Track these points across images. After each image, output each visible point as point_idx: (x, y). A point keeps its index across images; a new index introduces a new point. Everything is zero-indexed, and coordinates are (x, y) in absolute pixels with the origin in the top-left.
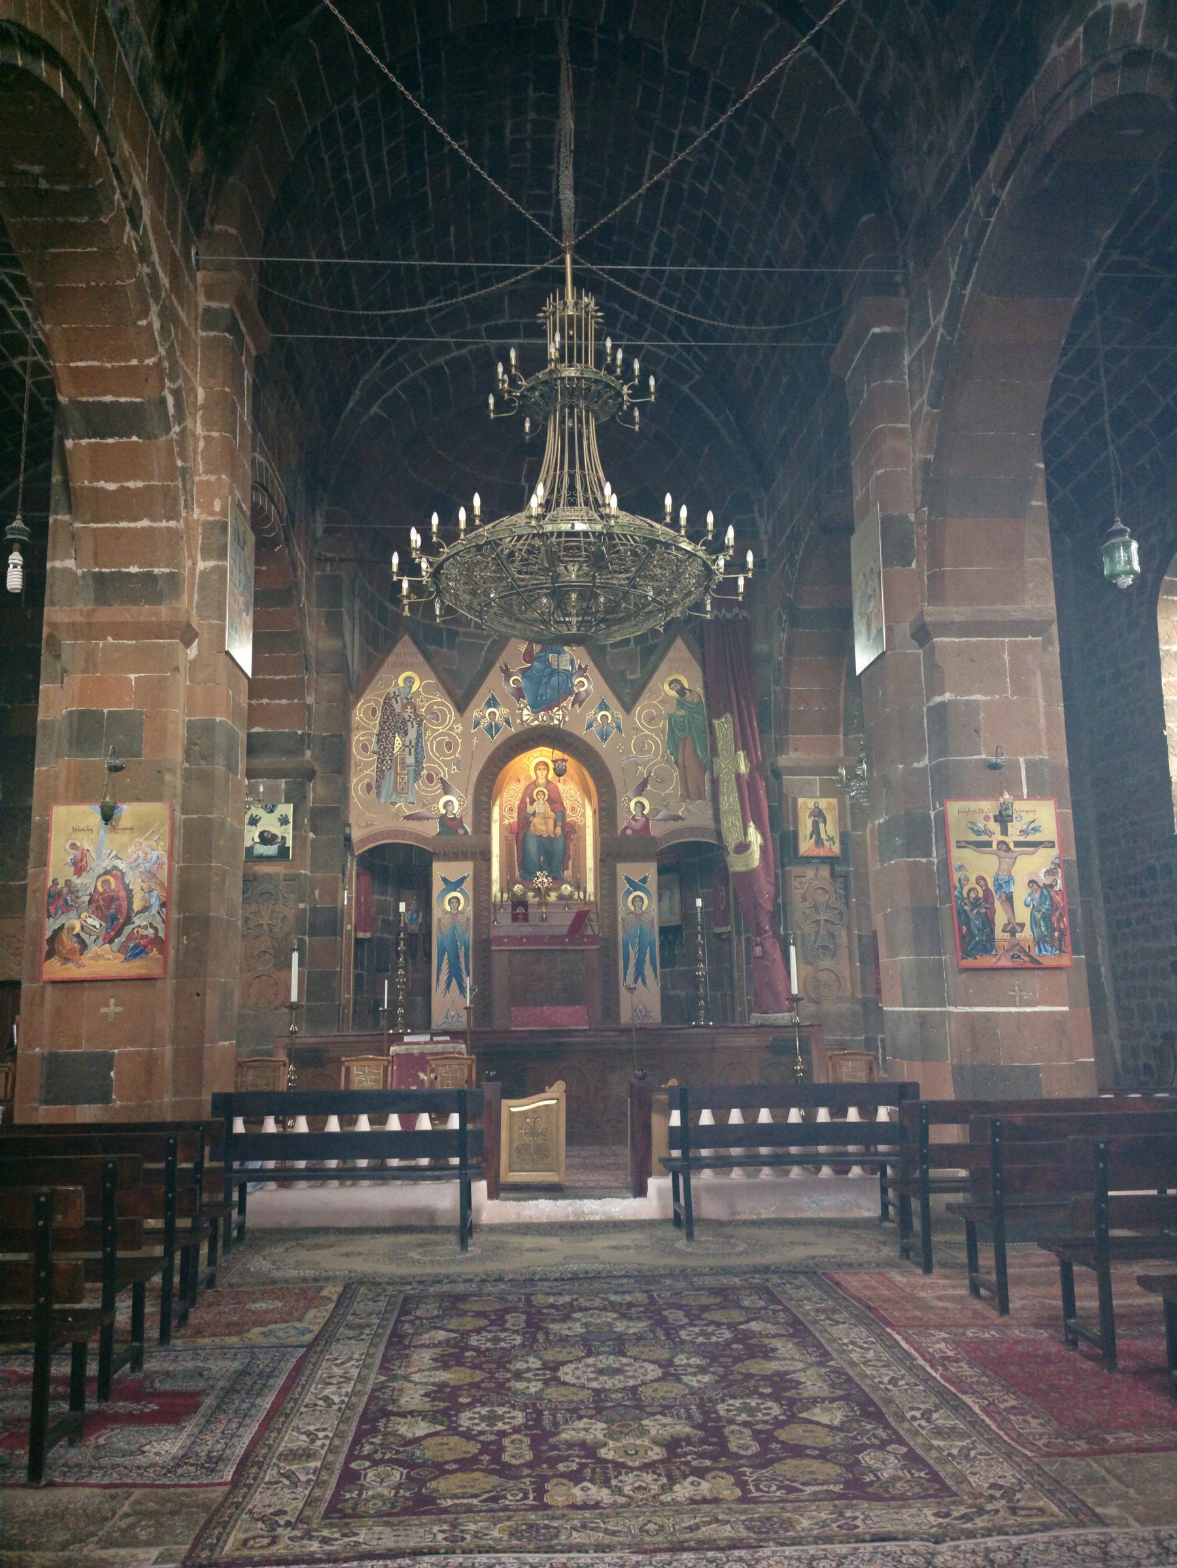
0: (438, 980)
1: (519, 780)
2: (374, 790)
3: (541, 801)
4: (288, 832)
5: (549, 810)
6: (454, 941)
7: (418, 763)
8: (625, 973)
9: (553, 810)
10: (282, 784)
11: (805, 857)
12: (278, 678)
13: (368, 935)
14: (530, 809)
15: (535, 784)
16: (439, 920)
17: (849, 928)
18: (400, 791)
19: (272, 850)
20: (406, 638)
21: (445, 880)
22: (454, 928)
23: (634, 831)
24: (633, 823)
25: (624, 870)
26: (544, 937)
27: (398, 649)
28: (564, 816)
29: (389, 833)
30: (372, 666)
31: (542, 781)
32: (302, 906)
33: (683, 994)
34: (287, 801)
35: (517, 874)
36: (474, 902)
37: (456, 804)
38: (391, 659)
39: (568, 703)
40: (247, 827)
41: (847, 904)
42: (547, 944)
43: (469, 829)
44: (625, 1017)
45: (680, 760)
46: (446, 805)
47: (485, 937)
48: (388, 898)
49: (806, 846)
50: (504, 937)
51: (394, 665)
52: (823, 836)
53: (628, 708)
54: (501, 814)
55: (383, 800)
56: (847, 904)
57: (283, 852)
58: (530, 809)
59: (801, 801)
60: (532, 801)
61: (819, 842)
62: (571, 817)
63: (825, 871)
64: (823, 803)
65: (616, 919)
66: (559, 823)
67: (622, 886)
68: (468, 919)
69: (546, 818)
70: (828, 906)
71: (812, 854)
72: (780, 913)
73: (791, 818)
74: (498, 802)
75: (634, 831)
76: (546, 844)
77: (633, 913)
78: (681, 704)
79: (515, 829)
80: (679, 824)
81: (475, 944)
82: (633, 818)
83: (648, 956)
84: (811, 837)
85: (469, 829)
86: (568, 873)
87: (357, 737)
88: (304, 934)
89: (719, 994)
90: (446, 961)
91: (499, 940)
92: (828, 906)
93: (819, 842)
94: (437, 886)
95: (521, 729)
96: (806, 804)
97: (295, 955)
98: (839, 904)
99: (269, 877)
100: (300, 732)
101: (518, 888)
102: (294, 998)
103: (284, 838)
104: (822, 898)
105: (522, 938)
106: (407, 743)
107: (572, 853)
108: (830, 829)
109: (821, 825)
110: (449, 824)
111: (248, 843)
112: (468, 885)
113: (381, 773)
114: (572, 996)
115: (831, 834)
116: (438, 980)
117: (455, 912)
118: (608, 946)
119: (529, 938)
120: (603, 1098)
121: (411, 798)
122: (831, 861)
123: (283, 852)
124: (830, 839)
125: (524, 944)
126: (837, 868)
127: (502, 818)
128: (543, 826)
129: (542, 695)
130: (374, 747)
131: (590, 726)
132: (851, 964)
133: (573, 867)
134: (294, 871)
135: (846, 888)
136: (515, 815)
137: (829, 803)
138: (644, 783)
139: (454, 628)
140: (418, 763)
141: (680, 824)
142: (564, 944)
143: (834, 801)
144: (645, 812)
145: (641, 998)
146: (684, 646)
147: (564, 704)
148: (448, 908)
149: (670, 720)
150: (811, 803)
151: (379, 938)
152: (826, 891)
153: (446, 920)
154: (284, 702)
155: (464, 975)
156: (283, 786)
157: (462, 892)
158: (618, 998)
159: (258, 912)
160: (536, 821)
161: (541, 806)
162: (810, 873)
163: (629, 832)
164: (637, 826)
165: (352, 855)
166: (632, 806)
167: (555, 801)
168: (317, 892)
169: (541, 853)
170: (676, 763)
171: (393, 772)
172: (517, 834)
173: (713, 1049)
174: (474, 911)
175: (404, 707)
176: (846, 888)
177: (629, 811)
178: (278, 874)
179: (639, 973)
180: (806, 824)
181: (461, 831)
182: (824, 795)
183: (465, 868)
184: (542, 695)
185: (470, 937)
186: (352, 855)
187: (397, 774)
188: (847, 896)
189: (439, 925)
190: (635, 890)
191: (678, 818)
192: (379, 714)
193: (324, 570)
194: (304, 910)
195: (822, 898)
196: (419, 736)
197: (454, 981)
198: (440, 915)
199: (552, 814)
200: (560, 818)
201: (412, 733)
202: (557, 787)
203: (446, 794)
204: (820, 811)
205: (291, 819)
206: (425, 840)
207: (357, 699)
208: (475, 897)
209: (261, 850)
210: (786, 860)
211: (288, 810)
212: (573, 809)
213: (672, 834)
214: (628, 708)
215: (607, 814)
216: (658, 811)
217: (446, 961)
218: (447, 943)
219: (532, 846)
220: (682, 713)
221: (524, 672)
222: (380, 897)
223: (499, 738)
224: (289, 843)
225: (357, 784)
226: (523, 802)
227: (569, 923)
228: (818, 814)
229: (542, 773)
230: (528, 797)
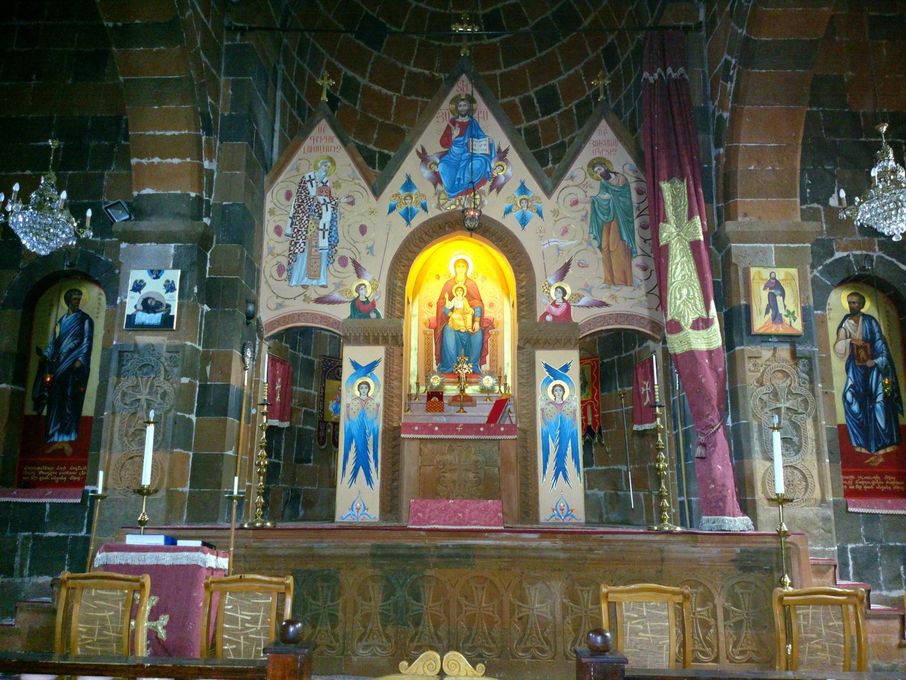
0: (344, 469)
1: (438, 277)
2: (285, 275)
3: (460, 297)
4: (173, 300)
5: (467, 305)
6: (363, 427)
7: (333, 245)
8: (545, 468)
9: (471, 306)
10: (171, 248)
11: (762, 335)
12: (169, 133)
13: (286, 424)
14: (449, 305)
15: (454, 281)
16: (348, 406)
17: (816, 420)
18: (313, 272)
19: (155, 318)
20: (324, 122)
21: (355, 365)
22: (363, 414)
23: (553, 316)
24: (554, 309)
25: (543, 357)
26: (457, 425)
27: (315, 133)
28: (482, 312)
29: (299, 316)
30: (289, 150)
31: (461, 278)
32: (185, 380)
33: (601, 494)
34: (175, 267)
35: (435, 367)
36: (385, 388)
37: (372, 287)
38: (308, 142)
39: (486, 188)
40: (131, 294)
41: (812, 390)
42: (461, 433)
43: (382, 313)
44: (546, 515)
45: (604, 246)
46: (357, 290)
47: (395, 425)
48: (312, 392)
49: (761, 322)
50: (415, 425)
51: (310, 149)
52: (782, 311)
53: (548, 193)
54: (420, 307)
55: (294, 283)
56: (812, 390)
57: (167, 321)
58: (449, 305)
59: (753, 271)
60: (451, 298)
61: (777, 318)
62: (489, 313)
63: (784, 351)
64: (781, 274)
65: (535, 406)
66: (478, 319)
67: (541, 374)
68: (378, 405)
69: (464, 313)
70: (790, 393)
71: (768, 332)
72: (731, 397)
73: (742, 290)
74: (417, 298)
75: (553, 316)
76: (464, 340)
77: (551, 402)
78: (605, 188)
79: (434, 322)
80: (603, 311)
81: (384, 432)
82: (554, 304)
83: (570, 449)
84: (767, 312)
85: (382, 313)
86: (485, 367)
87: (269, 223)
88: (191, 413)
89: (641, 494)
90: (353, 449)
91: (409, 427)
92: (790, 393)
93: (777, 318)
94: (347, 370)
95: (438, 212)
96: (759, 275)
97: (151, 430)
98: (805, 391)
99: (151, 348)
100: (193, 195)
101: (436, 381)
102: (146, 481)
103: (168, 306)
104: (782, 384)
105: (434, 425)
106: (321, 227)
107: (490, 348)
108: (790, 303)
109: (779, 299)
110: (361, 308)
111: (129, 310)
112: (379, 371)
113: (293, 256)
114: (488, 487)
115: (791, 308)
116: (344, 469)
117: (364, 398)
118: (527, 437)
119: (440, 426)
120: (520, 619)
121: (323, 282)
122: (791, 339)
123: (167, 321)
124: (790, 314)
125: (437, 433)
126: (799, 348)
127: (420, 313)
128: (462, 319)
129: (459, 179)
130: (289, 231)
131: (508, 211)
132: (819, 460)
133: (492, 361)
134: (177, 342)
135: (810, 372)
136: (434, 309)
137: (786, 273)
138: (565, 269)
139: (386, 152)
140: (333, 245)
141: (603, 311)
142: (479, 433)
143: (794, 271)
144: (566, 298)
145: (562, 493)
146: (609, 129)
147: (482, 188)
148: (358, 394)
149: (593, 203)
150: (766, 274)
151: (300, 430)
152: (786, 375)
153: (355, 405)
154: (176, 161)
155: (372, 465)
156: (172, 251)
157: (374, 378)
158: (537, 495)
159: (136, 387)
160: (454, 316)
161: (460, 302)
162: (766, 353)
163: (549, 318)
164: (558, 312)
165: (261, 338)
166: (548, 297)
167: (473, 297)
168: (208, 368)
169: (461, 349)
170: (600, 247)
171: (306, 254)
172: (436, 330)
173: (663, 560)
174: (385, 398)
175: (320, 192)
176: (810, 372)
177: (549, 296)
178: (160, 345)
179: (560, 468)
180: (760, 298)
181: (373, 315)
182: (780, 264)
183: (378, 352)
184: (459, 179)
185: (380, 425)
186: (261, 338)
187: (310, 254)
188: (811, 382)
189: (348, 411)
190: (555, 379)
191: (603, 304)
192: (294, 198)
193: (234, 40)
194: (191, 385)
195: (782, 384)
196: (333, 220)
197: (361, 470)
198: (349, 401)
199: (471, 310)
200: (478, 314)
201: (327, 217)
202: (475, 284)
203: (359, 276)
204: (777, 282)
205: (177, 287)
206: (336, 323)
207: (272, 182)
208: (386, 382)
209: (143, 318)
210: (736, 339)
211: (175, 276)
212: (491, 305)
213: (596, 320)
214: (548, 193)
215: (526, 301)
216: (580, 297)
217: (353, 449)
218: (355, 431)
219: (450, 341)
220: (607, 196)
221: (442, 156)
222: (303, 389)
223: (416, 222)
224: (174, 312)
225: (268, 266)
226: (442, 297)
227: (487, 414)
228: (775, 286)
229: (461, 270)
230: (448, 292)
